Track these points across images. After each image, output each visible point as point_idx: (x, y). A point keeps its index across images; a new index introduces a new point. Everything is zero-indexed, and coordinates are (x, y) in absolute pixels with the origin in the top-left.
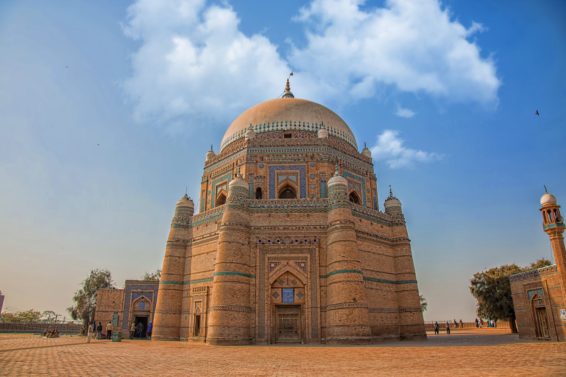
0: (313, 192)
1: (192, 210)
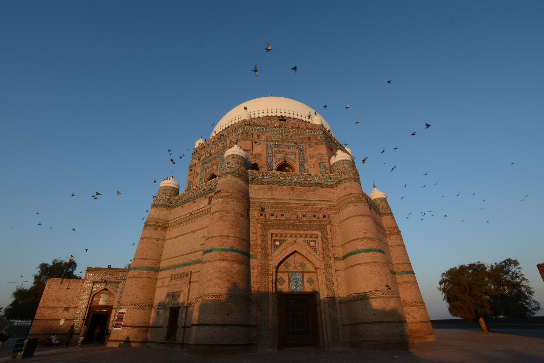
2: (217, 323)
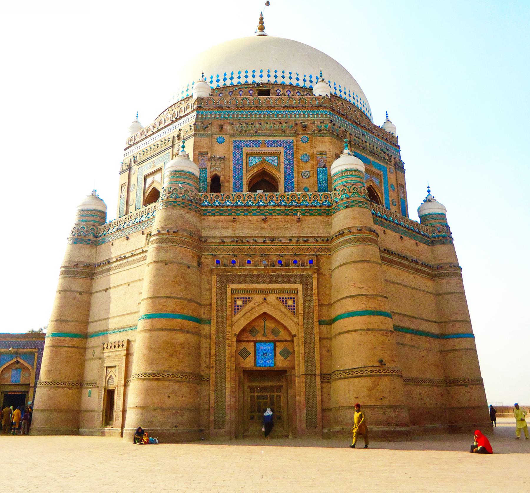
0: (305, 183)
1: (102, 215)
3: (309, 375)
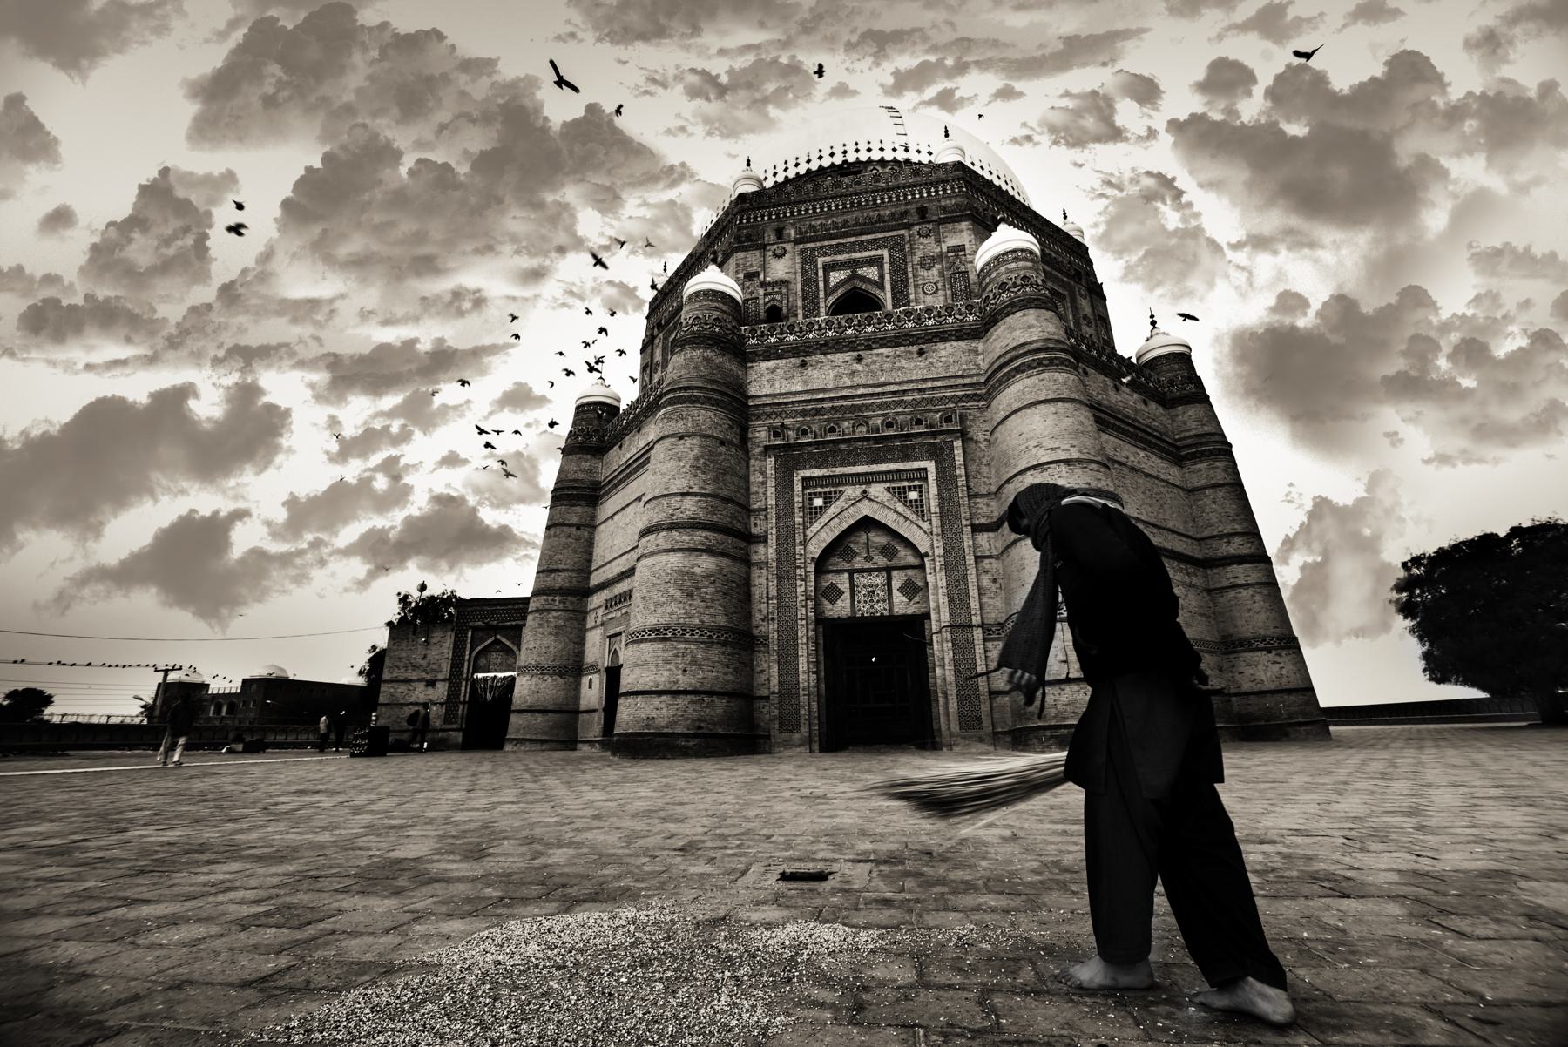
2: (660, 688)
3: (960, 627)
